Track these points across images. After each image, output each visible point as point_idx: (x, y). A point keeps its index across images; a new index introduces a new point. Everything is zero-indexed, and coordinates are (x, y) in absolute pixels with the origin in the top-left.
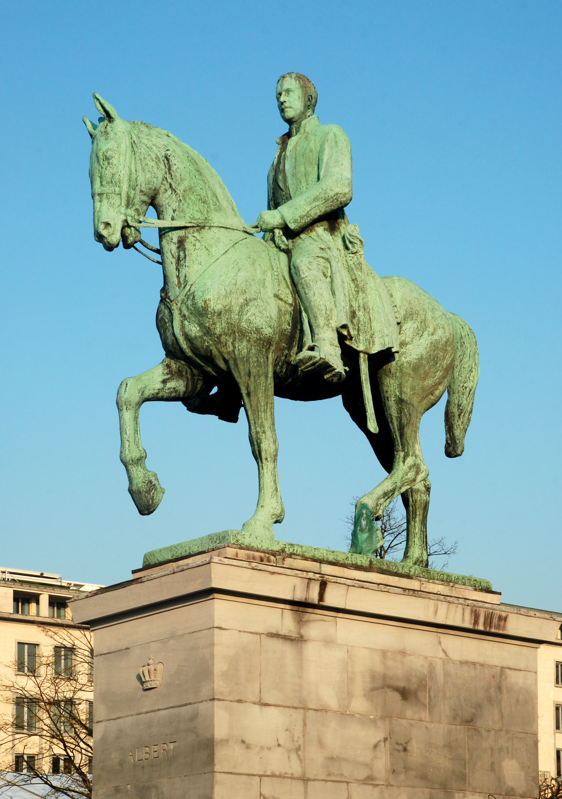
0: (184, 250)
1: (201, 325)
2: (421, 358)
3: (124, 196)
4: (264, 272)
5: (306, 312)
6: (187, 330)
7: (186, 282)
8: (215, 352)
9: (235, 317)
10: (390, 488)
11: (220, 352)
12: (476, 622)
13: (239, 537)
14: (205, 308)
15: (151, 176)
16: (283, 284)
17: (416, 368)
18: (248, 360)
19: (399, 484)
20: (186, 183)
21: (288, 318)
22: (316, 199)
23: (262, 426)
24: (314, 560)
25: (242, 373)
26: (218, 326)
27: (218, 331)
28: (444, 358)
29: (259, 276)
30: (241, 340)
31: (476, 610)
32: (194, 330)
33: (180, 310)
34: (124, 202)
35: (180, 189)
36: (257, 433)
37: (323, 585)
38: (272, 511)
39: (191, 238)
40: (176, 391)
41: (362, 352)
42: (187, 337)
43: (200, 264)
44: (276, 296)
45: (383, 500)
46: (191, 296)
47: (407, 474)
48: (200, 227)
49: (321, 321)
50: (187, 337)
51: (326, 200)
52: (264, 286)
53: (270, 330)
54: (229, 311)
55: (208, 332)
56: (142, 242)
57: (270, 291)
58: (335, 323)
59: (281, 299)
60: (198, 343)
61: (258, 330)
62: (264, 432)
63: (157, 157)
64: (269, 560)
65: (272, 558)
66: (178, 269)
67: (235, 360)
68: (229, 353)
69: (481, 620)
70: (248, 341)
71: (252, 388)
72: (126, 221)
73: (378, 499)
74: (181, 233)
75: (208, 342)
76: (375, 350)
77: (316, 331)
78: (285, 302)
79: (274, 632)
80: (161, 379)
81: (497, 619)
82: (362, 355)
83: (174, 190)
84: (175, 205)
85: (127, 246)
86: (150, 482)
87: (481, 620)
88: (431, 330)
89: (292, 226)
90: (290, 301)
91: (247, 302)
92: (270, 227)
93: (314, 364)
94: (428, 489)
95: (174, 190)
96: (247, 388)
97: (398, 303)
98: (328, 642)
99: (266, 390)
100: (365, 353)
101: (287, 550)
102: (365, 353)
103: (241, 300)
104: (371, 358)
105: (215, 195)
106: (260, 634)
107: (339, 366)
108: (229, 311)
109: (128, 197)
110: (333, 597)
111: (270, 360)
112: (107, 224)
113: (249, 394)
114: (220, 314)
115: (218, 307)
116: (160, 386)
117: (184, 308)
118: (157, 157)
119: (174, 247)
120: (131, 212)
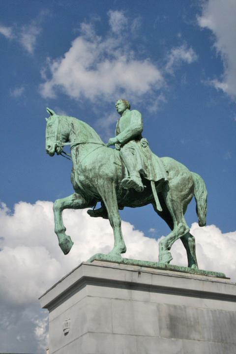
0: (78, 151)
1: (84, 176)
2: (178, 184)
3: (56, 136)
4: (110, 156)
5: (126, 166)
6: (80, 179)
7: (79, 162)
8: (91, 185)
9: (97, 170)
13: (101, 256)
14: (85, 169)
15: (65, 129)
16: (117, 159)
17: (177, 187)
18: (104, 187)
20: (79, 131)
21: (120, 171)
23: (113, 212)
24: (138, 265)
25: (102, 192)
26: (91, 174)
27: (91, 177)
28: (189, 184)
29: (107, 156)
30: (100, 179)
32: (82, 178)
34: (56, 139)
35: (77, 133)
36: (111, 215)
38: (120, 247)
41: (151, 180)
42: (81, 182)
43: (84, 155)
44: (115, 163)
46: (81, 166)
48: (84, 143)
49: (132, 169)
50: (81, 182)
52: (109, 160)
54: (94, 168)
55: (87, 178)
56: (63, 152)
57: (112, 160)
58: (139, 167)
59: (116, 164)
60: (84, 183)
62: (114, 215)
63: (69, 124)
66: (76, 159)
67: (99, 187)
70: (103, 179)
71: (107, 197)
72: (56, 145)
75: (88, 182)
76: (157, 180)
77: (130, 173)
78: (119, 165)
82: (152, 182)
83: (75, 133)
84: (75, 138)
85: (58, 154)
86: (67, 239)
88: (181, 173)
89: (121, 141)
90: (120, 164)
92: (113, 143)
93: (129, 183)
95: (75, 133)
96: (105, 197)
97: (166, 165)
98: (146, 302)
99: (113, 197)
100: (153, 181)
102: (153, 181)
103: (99, 164)
104: (156, 183)
105: (91, 134)
107: (140, 184)
108: (94, 168)
109: (57, 137)
111: (114, 186)
112: (49, 147)
113: (106, 200)
114: (91, 170)
115: (90, 167)
116: (71, 202)
117: (78, 171)
118: (69, 124)
120: (58, 141)
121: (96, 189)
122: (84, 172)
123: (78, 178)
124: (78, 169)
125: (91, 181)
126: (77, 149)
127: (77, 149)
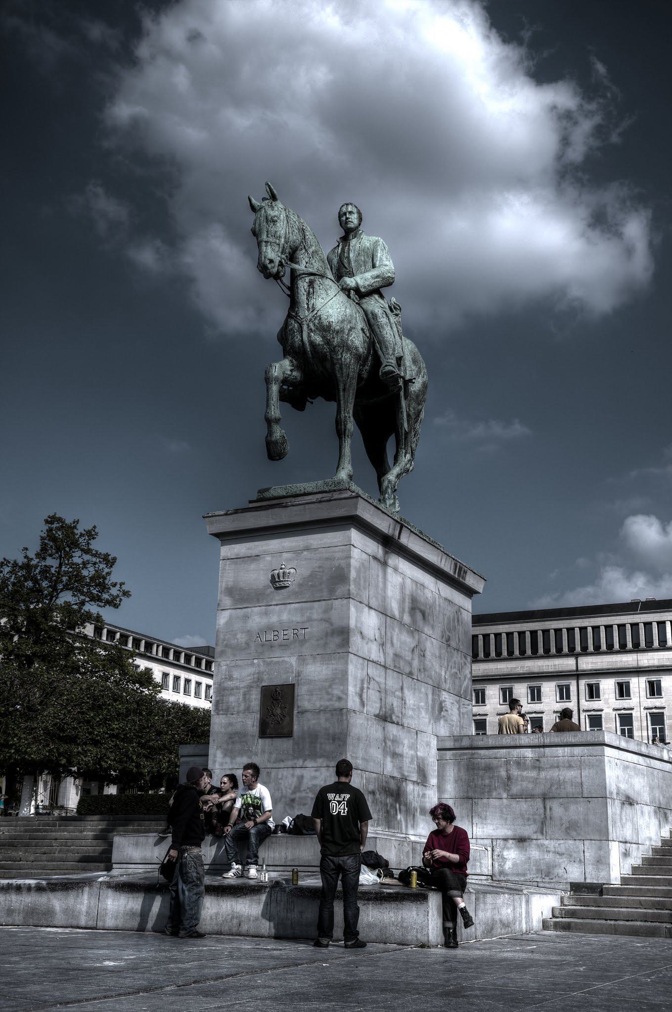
0: (313, 288)
8: (329, 357)
11: (332, 358)
22: (378, 277)
32: (318, 339)
33: (308, 325)
39: (318, 281)
42: (312, 343)
51: (383, 279)
68: (338, 359)
74: (312, 277)
75: (326, 349)
84: (307, 260)
89: (363, 290)
117: (311, 325)
119: (306, 285)
120: (283, 256)
121: (333, 364)
122: (325, 330)
123: (309, 336)
124: (311, 320)
125: (333, 350)
126: (311, 284)
127: (311, 284)
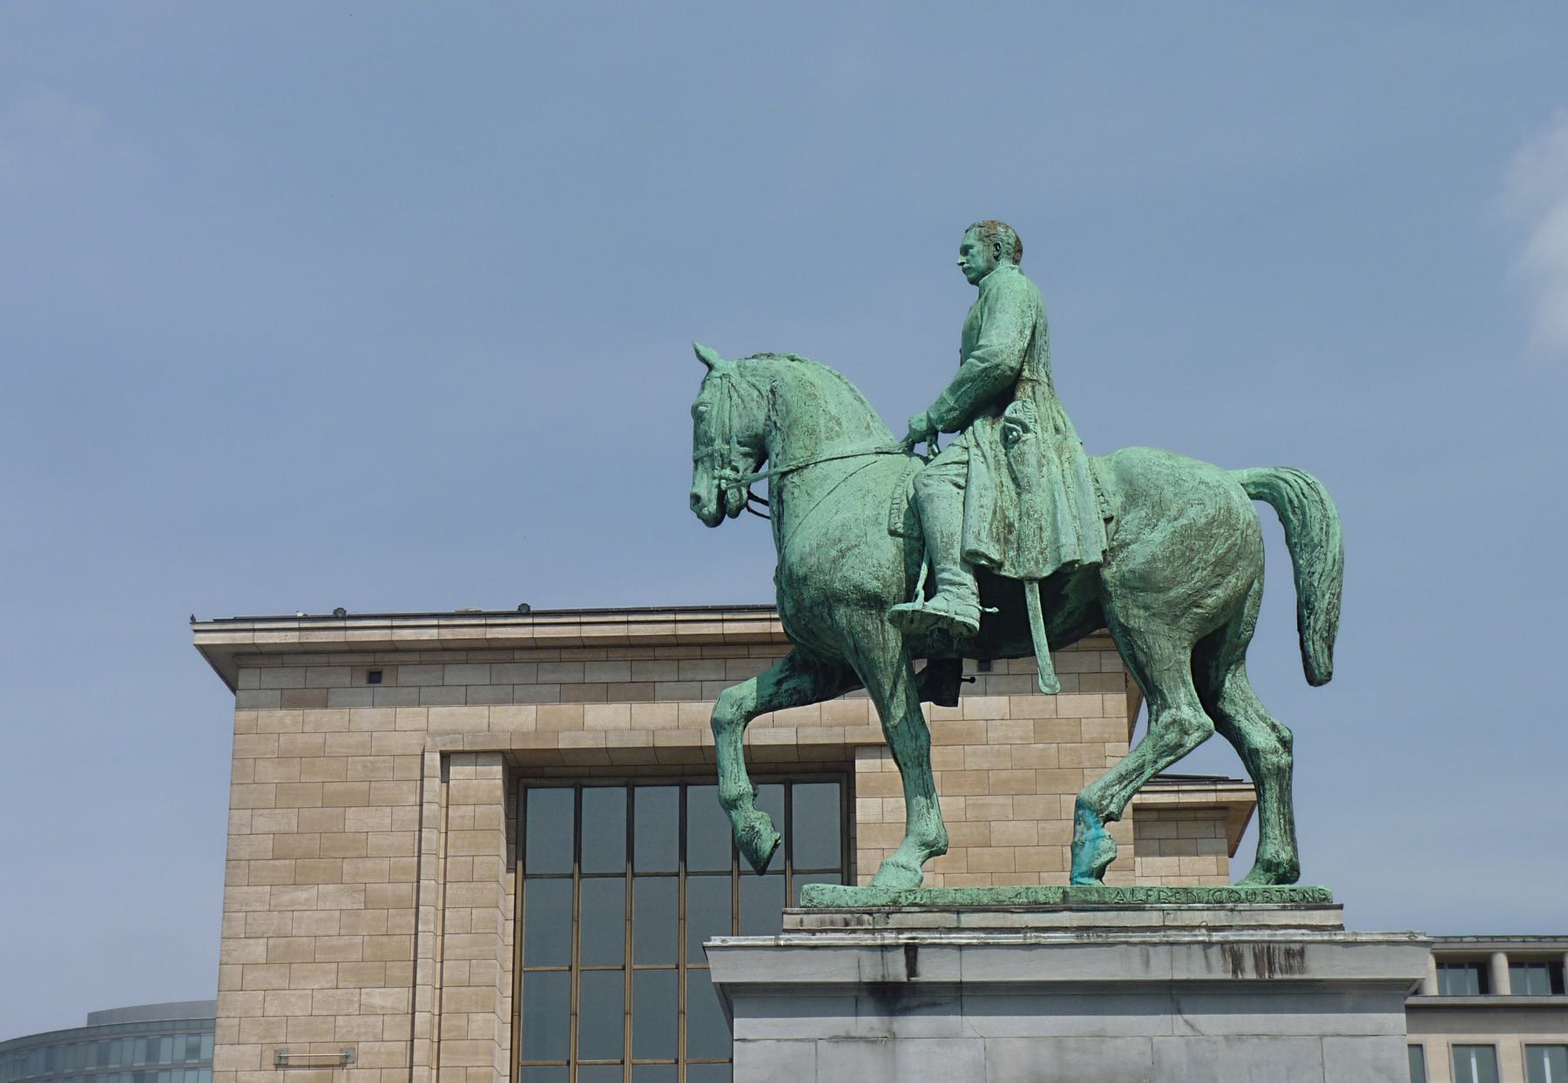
10: (1131, 767)
12: (1237, 966)
19: (1150, 757)
24: (945, 909)
31: (1231, 949)
37: (911, 950)
40: (799, 692)
45: (1117, 788)
47: (1162, 737)
53: (875, 583)
61: (858, 588)
64: (860, 922)
65: (866, 917)
69: (1249, 962)
73: (1107, 787)
79: (842, 1034)
80: (774, 680)
81: (1282, 956)
86: (753, 828)
87: (1249, 962)
91: (842, 553)
94: (1286, 744)
101: (903, 900)
106: (815, 1041)
110: (933, 970)
